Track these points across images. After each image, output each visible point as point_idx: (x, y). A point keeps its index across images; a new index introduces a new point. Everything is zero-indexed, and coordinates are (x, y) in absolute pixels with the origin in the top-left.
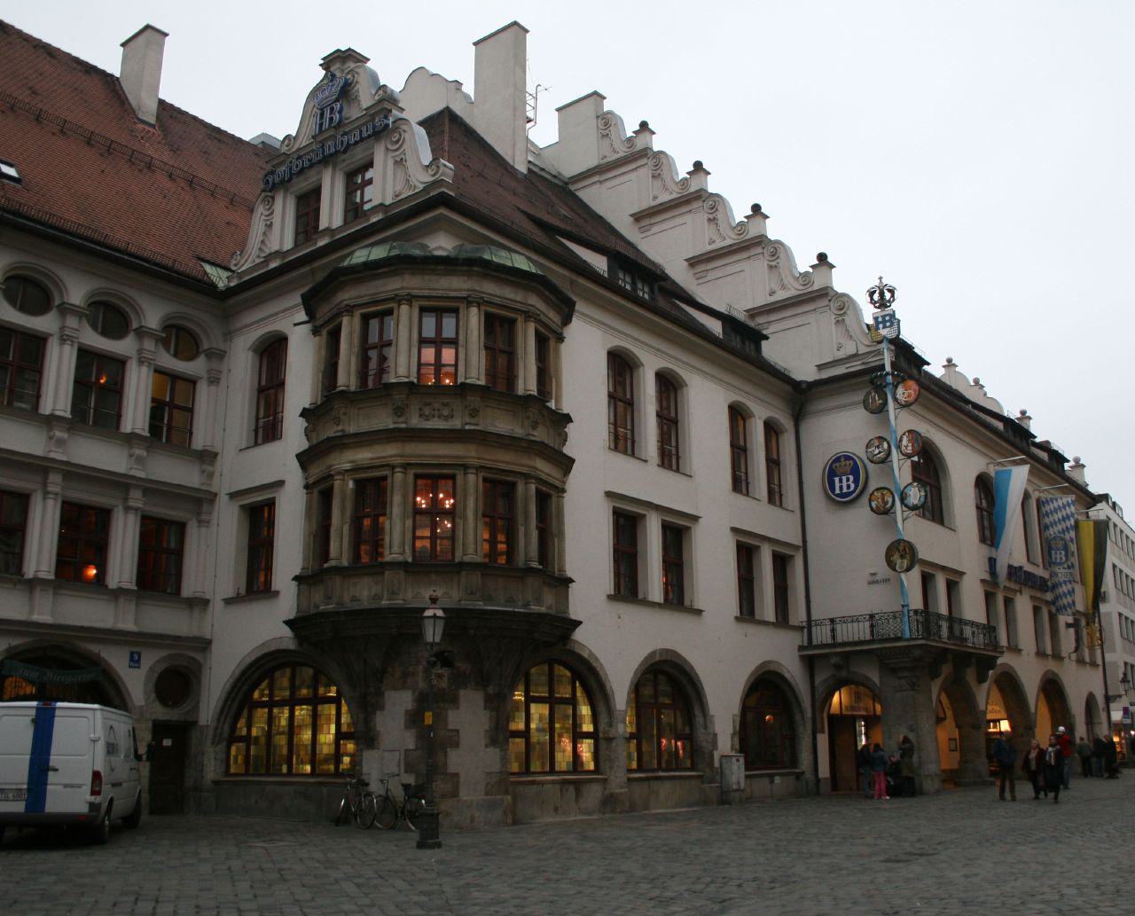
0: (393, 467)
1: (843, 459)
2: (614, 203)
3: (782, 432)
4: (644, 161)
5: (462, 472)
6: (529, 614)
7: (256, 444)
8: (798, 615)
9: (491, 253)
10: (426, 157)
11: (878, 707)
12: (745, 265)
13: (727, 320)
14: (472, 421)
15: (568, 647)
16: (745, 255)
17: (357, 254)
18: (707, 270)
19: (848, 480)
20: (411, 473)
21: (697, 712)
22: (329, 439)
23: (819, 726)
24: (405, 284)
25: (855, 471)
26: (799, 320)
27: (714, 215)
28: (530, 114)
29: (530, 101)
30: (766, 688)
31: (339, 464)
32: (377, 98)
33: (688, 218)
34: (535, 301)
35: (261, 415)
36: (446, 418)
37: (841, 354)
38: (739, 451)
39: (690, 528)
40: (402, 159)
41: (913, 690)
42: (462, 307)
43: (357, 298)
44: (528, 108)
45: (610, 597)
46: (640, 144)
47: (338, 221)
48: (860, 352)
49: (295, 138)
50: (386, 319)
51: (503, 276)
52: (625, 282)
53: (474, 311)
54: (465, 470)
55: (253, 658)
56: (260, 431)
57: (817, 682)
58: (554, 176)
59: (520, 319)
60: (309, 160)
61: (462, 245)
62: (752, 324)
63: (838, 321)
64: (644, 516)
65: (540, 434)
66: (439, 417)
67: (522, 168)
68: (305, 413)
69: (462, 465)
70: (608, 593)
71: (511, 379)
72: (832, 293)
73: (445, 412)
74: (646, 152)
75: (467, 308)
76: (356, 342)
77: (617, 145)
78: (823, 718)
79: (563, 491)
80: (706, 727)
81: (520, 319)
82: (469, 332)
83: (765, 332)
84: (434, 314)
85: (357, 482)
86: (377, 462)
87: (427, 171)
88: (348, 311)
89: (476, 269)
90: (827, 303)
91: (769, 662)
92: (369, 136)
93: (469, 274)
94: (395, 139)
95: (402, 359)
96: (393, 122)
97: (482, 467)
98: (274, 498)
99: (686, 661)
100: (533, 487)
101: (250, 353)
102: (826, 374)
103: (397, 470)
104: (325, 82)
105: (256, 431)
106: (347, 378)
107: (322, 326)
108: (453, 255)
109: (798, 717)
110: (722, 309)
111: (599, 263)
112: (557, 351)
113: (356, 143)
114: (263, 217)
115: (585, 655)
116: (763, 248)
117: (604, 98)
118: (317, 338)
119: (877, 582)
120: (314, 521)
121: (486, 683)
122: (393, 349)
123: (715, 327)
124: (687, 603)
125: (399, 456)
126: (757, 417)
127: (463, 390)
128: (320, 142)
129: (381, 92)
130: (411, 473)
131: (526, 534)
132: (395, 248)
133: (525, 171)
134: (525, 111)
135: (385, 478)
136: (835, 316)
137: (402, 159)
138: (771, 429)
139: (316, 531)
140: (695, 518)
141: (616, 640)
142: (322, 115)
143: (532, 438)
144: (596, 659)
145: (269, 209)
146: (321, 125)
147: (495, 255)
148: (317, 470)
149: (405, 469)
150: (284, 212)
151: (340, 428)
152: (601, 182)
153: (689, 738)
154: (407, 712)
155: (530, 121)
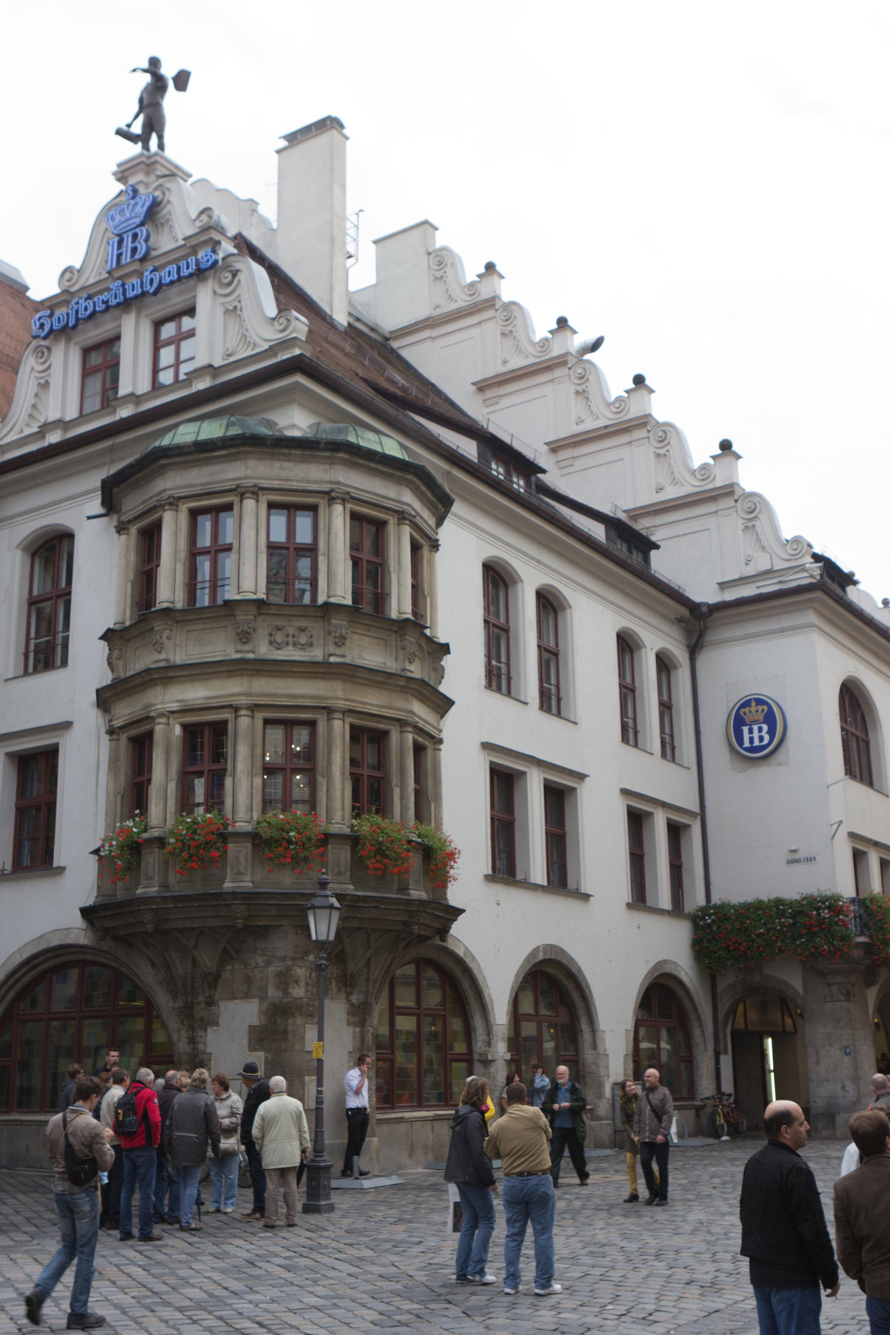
0: (236, 709)
1: (753, 704)
2: (450, 366)
3: (676, 668)
4: (490, 314)
5: (325, 717)
6: (409, 902)
7: (26, 673)
8: (696, 898)
9: (357, 435)
10: (271, 310)
11: (789, 1021)
12: (624, 453)
13: (616, 526)
14: (338, 651)
15: (444, 944)
16: (625, 438)
17: (182, 429)
18: (574, 458)
19: (760, 730)
20: (260, 716)
21: (584, 1026)
22: (148, 671)
23: (722, 1045)
24: (249, 473)
25: (770, 719)
26: (696, 525)
27: (583, 387)
28: (351, 248)
29: (351, 232)
30: (660, 998)
31: (163, 703)
32: (198, 224)
33: (548, 390)
34: (408, 499)
35: (33, 635)
36: (303, 647)
37: (750, 571)
38: (628, 692)
39: (573, 790)
40: (235, 307)
41: (848, 1000)
42: (322, 503)
43: (184, 487)
44: (348, 239)
45: (487, 877)
46: (485, 293)
47: (144, 386)
48: (775, 568)
49: (78, 271)
50: (222, 515)
51: (372, 465)
52: (497, 470)
53: (338, 509)
54: (328, 713)
55: (26, 955)
56: (31, 656)
57: (723, 984)
58: (373, 330)
59: (392, 521)
60: (103, 302)
61: (319, 424)
62: (637, 526)
63: (747, 527)
64: (523, 774)
65: (416, 670)
66: (294, 645)
67: (341, 318)
68: (108, 636)
69: (324, 708)
70: (486, 873)
71: (380, 600)
72: (738, 493)
73: (303, 639)
74: (491, 303)
75: (329, 505)
76: (183, 543)
77: (456, 292)
78: (725, 1035)
79: (440, 741)
80: (594, 1046)
81: (392, 521)
82: (332, 536)
83: (653, 538)
84: (285, 512)
85: (185, 727)
86: (213, 703)
87: (273, 326)
88: (171, 504)
89: (341, 455)
90: (733, 504)
91: (665, 962)
92: (191, 275)
93: (331, 462)
94: (225, 281)
95: (248, 570)
96: (223, 259)
97: (350, 711)
98: (57, 745)
99: (572, 959)
100: (410, 737)
101: (19, 553)
102: (730, 595)
103: (243, 712)
104: (123, 198)
105: (26, 655)
106: (169, 589)
107: (130, 521)
108: (310, 435)
109: (697, 1033)
110: (605, 508)
111: (469, 448)
112: (431, 563)
113: (172, 283)
114: (34, 374)
115: (460, 952)
116: (649, 431)
117: (436, 229)
118: (123, 537)
119: (797, 861)
120: (122, 777)
121: (349, 990)
122: (233, 555)
123: (598, 531)
124: (571, 884)
125: (246, 695)
126: (648, 648)
127: (329, 608)
128: (118, 278)
129: (204, 218)
130: (260, 716)
131: (402, 797)
132: (234, 424)
133: (346, 324)
134: (344, 243)
135: (225, 722)
136: (744, 521)
137: (235, 307)
138: (664, 664)
139: (124, 789)
140: (581, 777)
141: (496, 933)
142: (120, 242)
143: (409, 674)
144: (473, 957)
145: (43, 363)
146: (119, 256)
147: (362, 438)
148: (124, 712)
149: (253, 711)
150: (66, 363)
151: (163, 656)
152: (433, 339)
153: (575, 1063)
154: (252, 1028)
155: (350, 257)
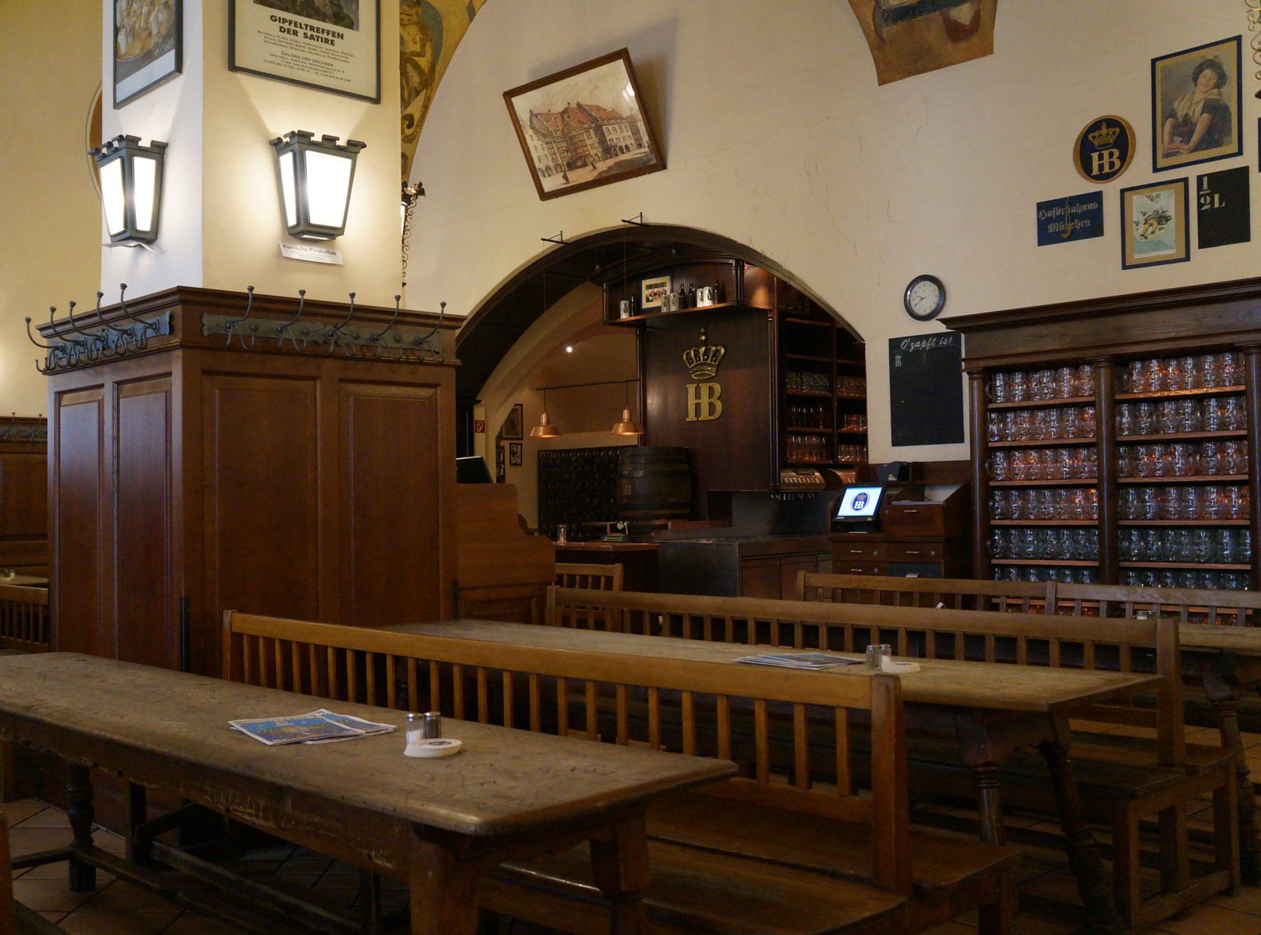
1: (1104, 125)
